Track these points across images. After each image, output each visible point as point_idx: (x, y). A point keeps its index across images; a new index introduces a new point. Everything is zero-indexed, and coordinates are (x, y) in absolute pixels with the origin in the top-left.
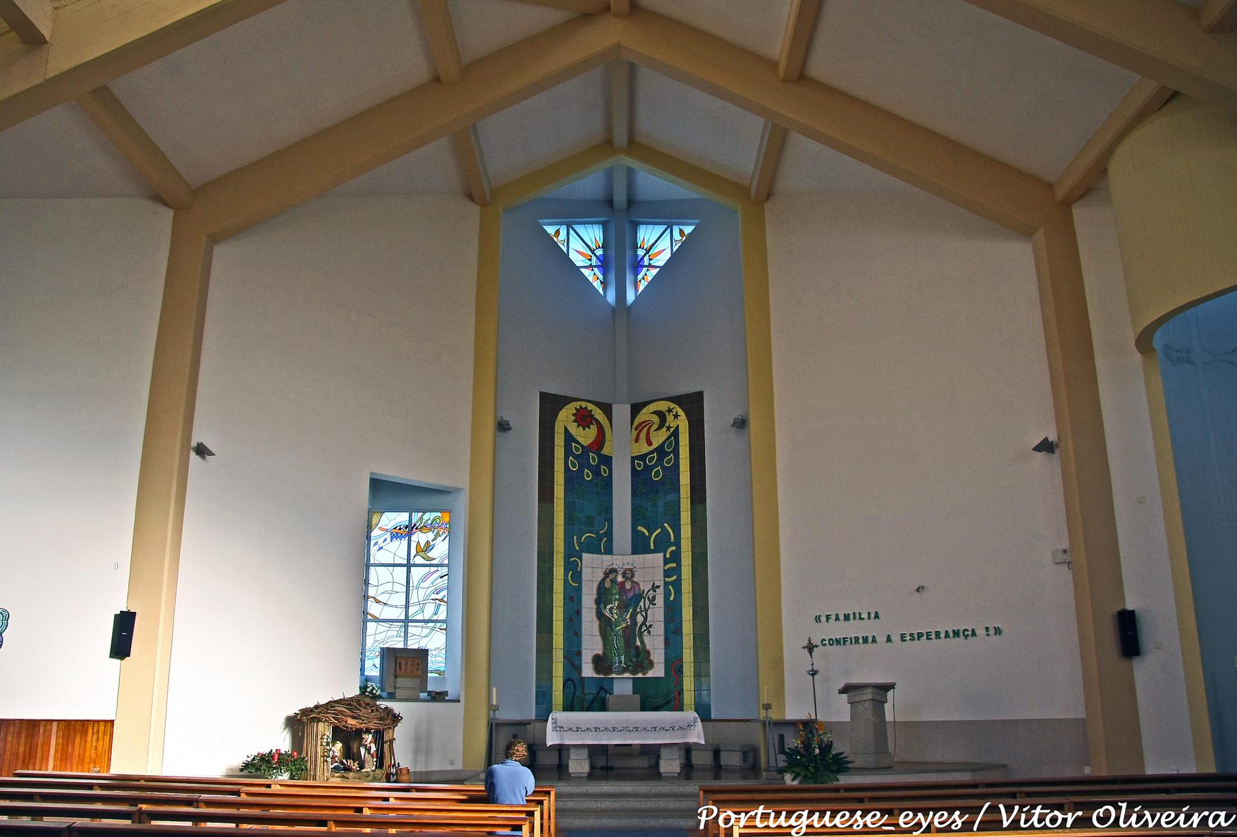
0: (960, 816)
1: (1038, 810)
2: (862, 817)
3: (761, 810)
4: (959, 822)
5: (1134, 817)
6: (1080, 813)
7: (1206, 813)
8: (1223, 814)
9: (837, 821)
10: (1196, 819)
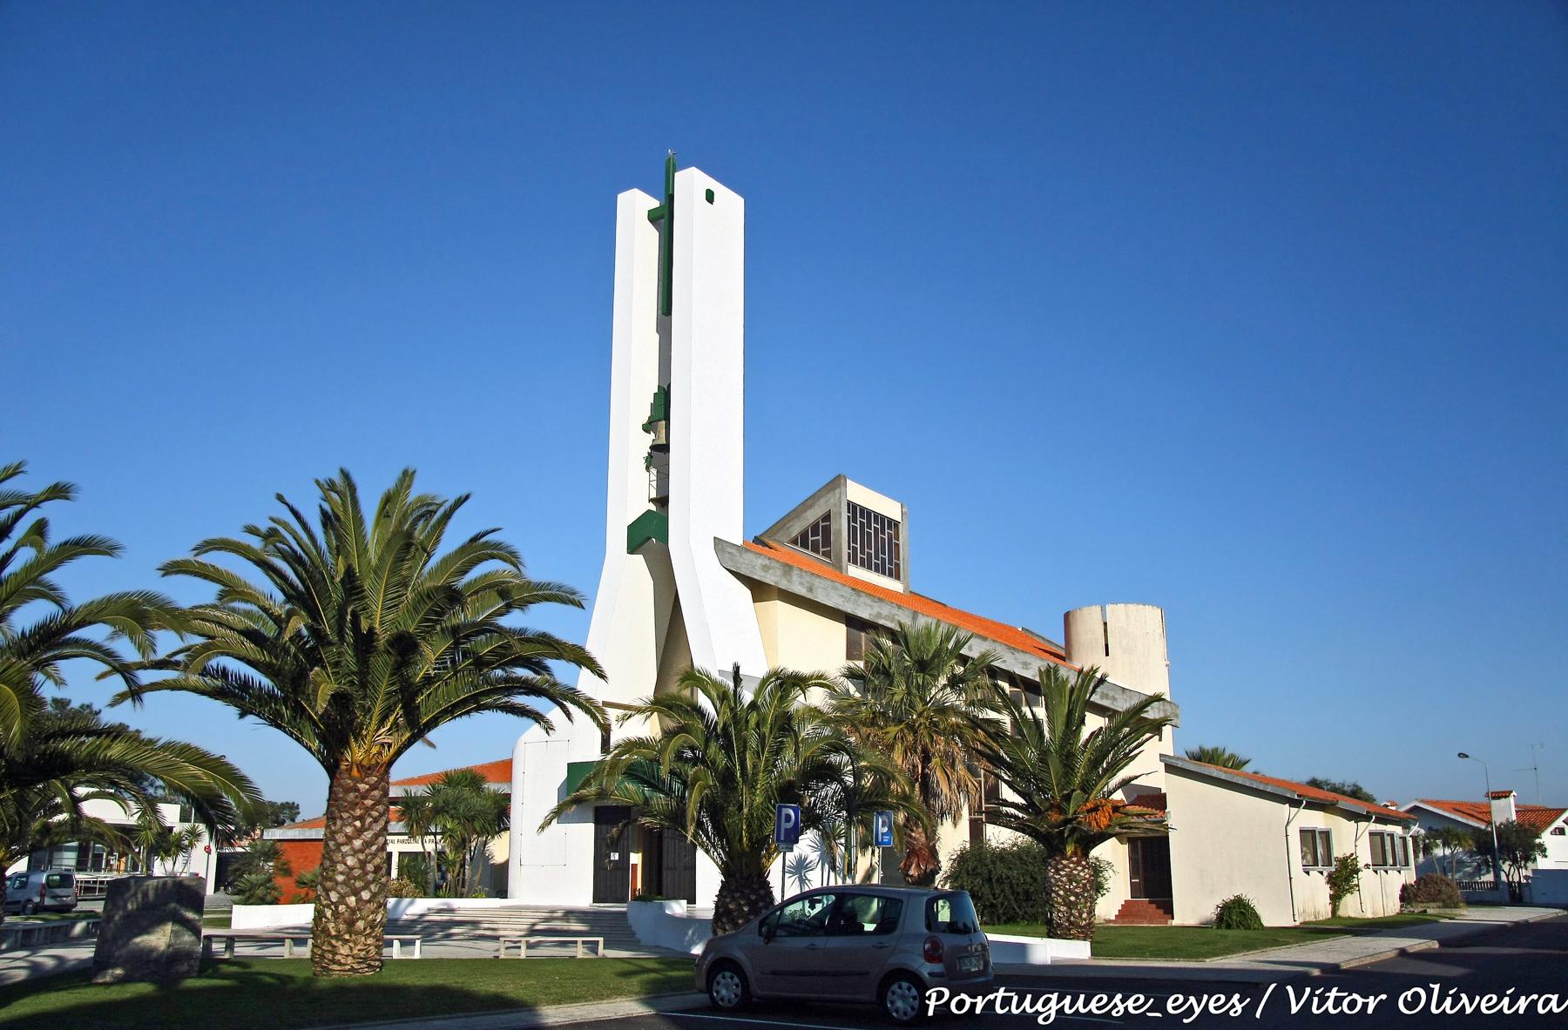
0: (1241, 1001)
1: (1334, 993)
2: (1123, 1001)
3: (1001, 993)
4: (1239, 1008)
5: (1449, 1001)
6: (1384, 997)
7: (1535, 997)
8: (1555, 998)
9: (1093, 1006)
10: (1522, 1004)
